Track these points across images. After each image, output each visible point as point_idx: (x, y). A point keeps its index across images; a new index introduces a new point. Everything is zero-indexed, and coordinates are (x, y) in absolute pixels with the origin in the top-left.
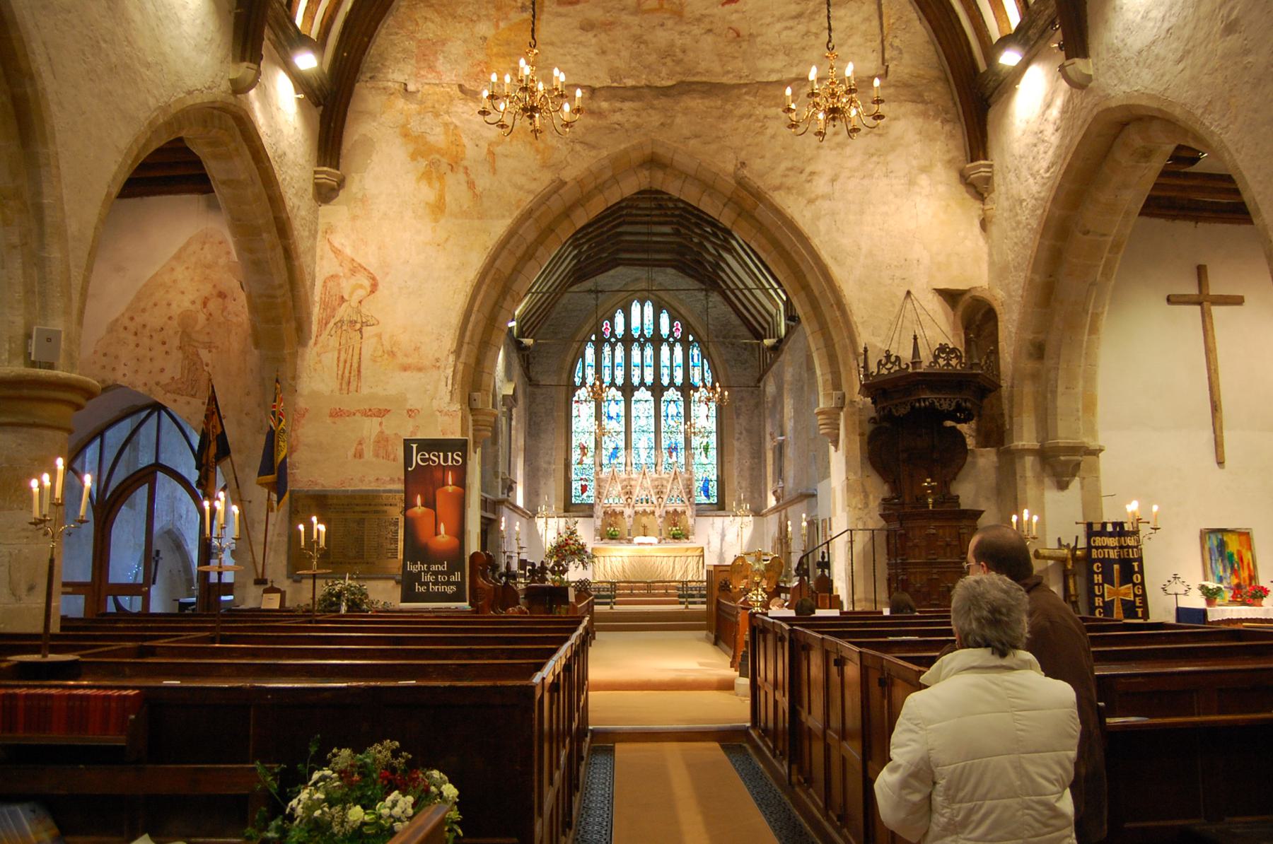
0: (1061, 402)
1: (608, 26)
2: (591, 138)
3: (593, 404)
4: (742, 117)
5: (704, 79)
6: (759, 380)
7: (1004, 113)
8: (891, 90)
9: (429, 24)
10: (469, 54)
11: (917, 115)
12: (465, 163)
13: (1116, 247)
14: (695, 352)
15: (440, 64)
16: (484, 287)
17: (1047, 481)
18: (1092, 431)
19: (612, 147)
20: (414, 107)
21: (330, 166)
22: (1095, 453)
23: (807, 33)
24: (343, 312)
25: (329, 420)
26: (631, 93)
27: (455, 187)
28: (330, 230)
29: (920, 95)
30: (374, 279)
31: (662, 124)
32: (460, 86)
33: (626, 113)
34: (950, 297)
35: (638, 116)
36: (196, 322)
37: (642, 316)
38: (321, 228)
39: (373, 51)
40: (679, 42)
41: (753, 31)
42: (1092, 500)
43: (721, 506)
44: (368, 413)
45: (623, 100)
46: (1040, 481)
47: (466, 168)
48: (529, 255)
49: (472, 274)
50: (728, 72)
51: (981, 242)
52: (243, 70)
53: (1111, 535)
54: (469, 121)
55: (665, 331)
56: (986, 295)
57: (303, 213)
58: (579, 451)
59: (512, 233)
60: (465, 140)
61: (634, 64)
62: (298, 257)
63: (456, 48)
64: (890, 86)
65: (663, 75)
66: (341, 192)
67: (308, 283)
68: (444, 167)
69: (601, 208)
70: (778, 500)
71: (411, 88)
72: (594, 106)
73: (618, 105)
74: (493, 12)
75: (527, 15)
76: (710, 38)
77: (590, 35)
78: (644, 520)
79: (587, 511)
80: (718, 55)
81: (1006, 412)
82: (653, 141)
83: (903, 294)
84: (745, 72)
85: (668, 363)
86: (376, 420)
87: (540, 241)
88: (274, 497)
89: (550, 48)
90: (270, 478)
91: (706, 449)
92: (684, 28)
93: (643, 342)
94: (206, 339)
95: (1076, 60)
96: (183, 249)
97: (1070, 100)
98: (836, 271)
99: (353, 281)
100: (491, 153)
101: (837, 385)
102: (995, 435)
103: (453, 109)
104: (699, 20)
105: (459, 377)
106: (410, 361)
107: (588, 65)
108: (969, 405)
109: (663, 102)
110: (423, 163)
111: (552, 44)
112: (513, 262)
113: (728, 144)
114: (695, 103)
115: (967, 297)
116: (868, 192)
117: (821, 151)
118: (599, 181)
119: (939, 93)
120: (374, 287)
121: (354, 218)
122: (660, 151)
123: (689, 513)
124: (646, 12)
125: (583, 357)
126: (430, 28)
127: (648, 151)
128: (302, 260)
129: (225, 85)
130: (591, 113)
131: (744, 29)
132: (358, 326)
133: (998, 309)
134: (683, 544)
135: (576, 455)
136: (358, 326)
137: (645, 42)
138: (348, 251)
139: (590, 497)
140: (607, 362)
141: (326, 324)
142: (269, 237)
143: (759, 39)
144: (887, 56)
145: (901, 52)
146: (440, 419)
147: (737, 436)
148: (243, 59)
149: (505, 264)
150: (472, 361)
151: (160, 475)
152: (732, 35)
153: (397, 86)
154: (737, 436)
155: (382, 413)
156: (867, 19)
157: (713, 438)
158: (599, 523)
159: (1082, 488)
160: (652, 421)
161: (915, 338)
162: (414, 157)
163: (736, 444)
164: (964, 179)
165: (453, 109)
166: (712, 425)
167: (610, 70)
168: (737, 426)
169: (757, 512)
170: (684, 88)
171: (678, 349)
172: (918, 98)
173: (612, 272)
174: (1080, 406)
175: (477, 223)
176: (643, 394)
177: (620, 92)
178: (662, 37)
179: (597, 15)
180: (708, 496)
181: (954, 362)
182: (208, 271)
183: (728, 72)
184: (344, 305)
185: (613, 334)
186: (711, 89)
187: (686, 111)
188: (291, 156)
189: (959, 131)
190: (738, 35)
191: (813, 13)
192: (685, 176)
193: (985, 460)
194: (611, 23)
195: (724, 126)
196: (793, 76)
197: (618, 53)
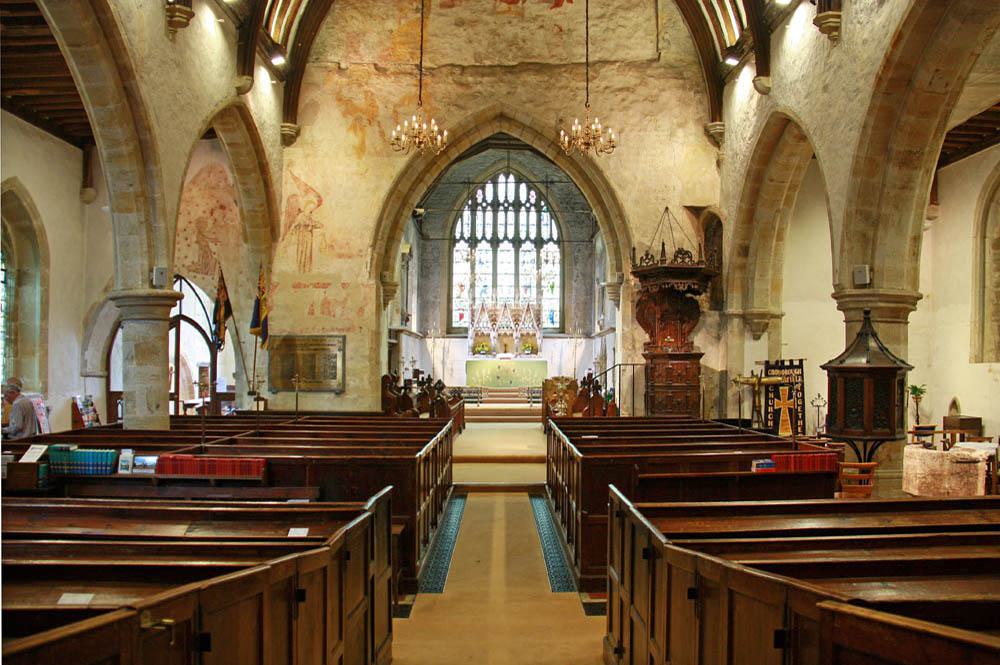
0: (756, 284)
1: (473, 23)
2: (461, 102)
4: (561, 88)
5: (537, 61)
6: (592, 237)
7: (731, 93)
8: (662, 70)
9: (355, 21)
10: (381, 43)
11: (679, 88)
12: (379, 119)
13: (793, 187)
14: (546, 216)
15: (362, 49)
16: (391, 203)
17: (747, 335)
18: (777, 302)
19: (475, 108)
20: (344, 80)
21: (291, 122)
22: (779, 317)
23: (607, 29)
24: (300, 219)
25: (292, 291)
26: (487, 71)
27: (371, 133)
28: (291, 164)
29: (681, 74)
30: (319, 197)
31: (509, 93)
32: (375, 65)
33: (484, 85)
34: (695, 211)
35: (493, 87)
36: (206, 225)
37: (506, 188)
38: (285, 163)
39: (318, 40)
40: (520, 35)
41: (572, 28)
42: (775, 345)
43: (562, 330)
44: (317, 286)
45: (483, 75)
46: (742, 334)
47: (379, 122)
48: (420, 180)
49: (383, 194)
50: (553, 56)
51: (717, 176)
52: (244, 80)
53: (788, 368)
54: (381, 90)
55: (523, 199)
56: (717, 212)
57: (275, 156)
58: (458, 288)
59: (409, 166)
60: (378, 103)
61: (490, 50)
62: (272, 187)
63: (373, 38)
64: (661, 67)
65: (510, 57)
66: (298, 139)
67: (278, 201)
68: (365, 122)
69: (468, 146)
70: (601, 329)
71: (343, 66)
72: (463, 79)
73: (479, 79)
74: (397, 12)
75: (419, 15)
76: (542, 32)
77: (462, 29)
78: (505, 340)
79: (462, 333)
80: (548, 44)
81: (725, 289)
82: (502, 105)
83: (662, 209)
84: (565, 55)
86: (322, 290)
87: (427, 170)
88: (260, 340)
89: (434, 38)
90: (258, 329)
91: (552, 287)
92: (525, 25)
94: (214, 237)
95: (762, 78)
96: (197, 176)
97: (760, 100)
98: (620, 194)
99: (306, 199)
100: (395, 112)
101: (619, 268)
102: (718, 303)
103: (370, 81)
104: (535, 19)
105: (374, 262)
106: (343, 251)
107: (460, 50)
108: (696, 287)
109: (510, 77)
110: (351, 119)
111: (436, 35)
112: (409, 184)
113: (551, 106)
114: (531, 78)
115: (706, 211)
116: (642, 141)
117: (614, 113)
118: (466, 131)
119: (694, 72)
120: (320, 202)
121: (307, 156)
122: (506, 111)
124: (499, 13)
125: (461, 216)
126: (356, 23)
127: (498, 111)
128: (275, 187)
129: (233, 92)
130: (461, 84)
131: (565, 27)
132: (310, 228)
133: (723, 222)
134: (534, 358)
135: (456, 292)
136: (310, 228)
137: (499, 35)
138: (303, 179)
139: (465, 323)
141: (290, 227)
142: (256, 175)
143: (575, 33)
144: (660, 46)
145: (669, 43)
146: (363, 289)
147: (575, 278)
148: (244, 74)
149: (404, 188)
150: (383, 251)
151: (182, 322)
152: (556, 29)
153: (333, 65)
154: (575, 278)
155: (325, 286)
156: (649, 20)
159: (769, 339)
160: (513, 265)
161: (663, 244)
162: (345, 114)
163: (574, 284)
164: (707, 132)
165: (370, 81)
167: (475, 54)
169: (588, 335)
170: (524, 67)
172: (679, 76)
173: (484, 153)
174: (769, 288)
175: (386, 159)
176: (506, 246)
177: (480, 70)
178: (509, 31)
179: (466, 15)
180: (553, 322)
181: (687, 260)
182: (213, 192)
183: (553, 56)
184: (301, 214)
185: (484, 200)
186: (541, 68)
187: (524, 84)
188: (268, 121)
189: (706, 99)
190: (561, 30)
191: (612, 15)
192: (522, 126)
193: (711, 318)
194: (475, 22)
195: (549, 95)
196: (596, 59)
197: (480, 42)
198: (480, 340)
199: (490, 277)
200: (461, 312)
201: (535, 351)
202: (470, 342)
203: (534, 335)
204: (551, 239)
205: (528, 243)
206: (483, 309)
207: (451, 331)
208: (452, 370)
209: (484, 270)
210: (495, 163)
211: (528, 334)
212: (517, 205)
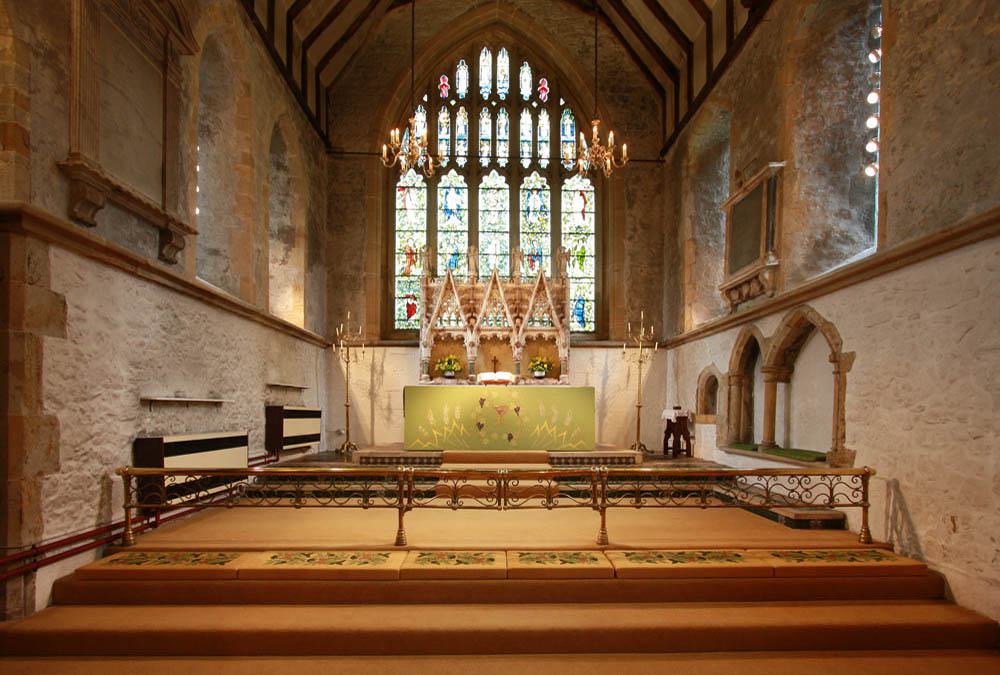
3: (424, 192)
14: (567, 121)
37: (494, 69)
43: (602, 335)
55: (526, 91)
79: (410, 339)
85: (529, 137)
93: (495, 105)
123: (561, 340)
135: (400, 263)
140: (444, 134)
147: (629, 232)
157: (591, 240)
160: (506, 217)
163: (626, 243)
166: (589, 223)
168: (629, 219)
171: (544, 119)
176: (494, 179)
180: (583, 322)
185: (453, 93)
198: (445, 349)
200: (410, 301)
201: (554, 371)
202: (424, 353)
203: (553, 340)
205: (535, 176)
206: (449, 287)
207: (389, 335)
209: (453, 225)
210: (472, 9)
211: (540, 337)
212: (514, 104)
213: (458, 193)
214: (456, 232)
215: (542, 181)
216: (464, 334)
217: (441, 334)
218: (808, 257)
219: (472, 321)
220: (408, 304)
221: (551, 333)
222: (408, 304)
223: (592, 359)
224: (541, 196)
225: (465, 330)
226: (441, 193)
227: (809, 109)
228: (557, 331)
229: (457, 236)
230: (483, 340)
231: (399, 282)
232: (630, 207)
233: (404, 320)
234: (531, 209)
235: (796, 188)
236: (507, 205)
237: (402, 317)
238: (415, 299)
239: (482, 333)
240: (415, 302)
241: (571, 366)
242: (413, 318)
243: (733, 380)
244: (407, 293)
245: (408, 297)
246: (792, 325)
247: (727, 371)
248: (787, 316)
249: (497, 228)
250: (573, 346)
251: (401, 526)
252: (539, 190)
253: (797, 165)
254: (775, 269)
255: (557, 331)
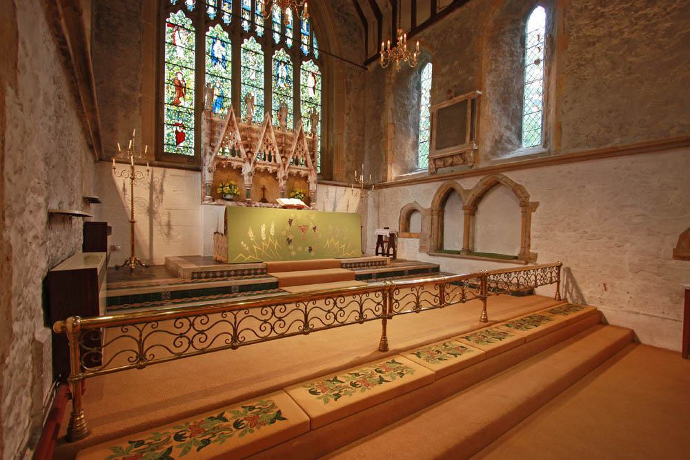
3: (193, 36)
58: (173, 89)
78: (264, 181)
135: (169, 94)
139: (187, 147)
158: (209, 177)
163: (346, 117)
166: (317, 97)
198: (225, 176)
199: (229, 84)
200: (180, 130)
203: (306, 178)
204: (310, 56)
205: (281, 51)
207: (161, 159)
208: (169, 225)
213: (223, 46)
214: (221, 77)
215: (287, 57)
216: (243, 165)
217: (223, 162)
218: (492, 147)
219: (250, 155)
220: (177, 131)
221: (306, 172)
222: (177, 131)
223: (327, 193)
224: (286, 67)
225: (244, 162)
226: (208, 41)
227: (494, 66)
228: (310, 170)
229: (222, 81)
230: (257, 171)
231: (168, 110)
232: (348, 93)
233: (172, 145)
234: (280, 76)
235: (487, 108)
236: (262, 67)
237: (171, 142)
238: (184, 128)
239: (258, 166)
240: (184, 131)
241: (319, 196)
242: (182, 144)
243: (435, 213)
244: (177, 121)
245: (177, 125)
246: (488, 184)
247: (430, 206)
248: (484, 179)
249: (255, 83)
250: (318, 183)
251: (384, 333)
252: (285, 64)
253: (488, 96)
254: (476, 151)
255: (310, 170)
